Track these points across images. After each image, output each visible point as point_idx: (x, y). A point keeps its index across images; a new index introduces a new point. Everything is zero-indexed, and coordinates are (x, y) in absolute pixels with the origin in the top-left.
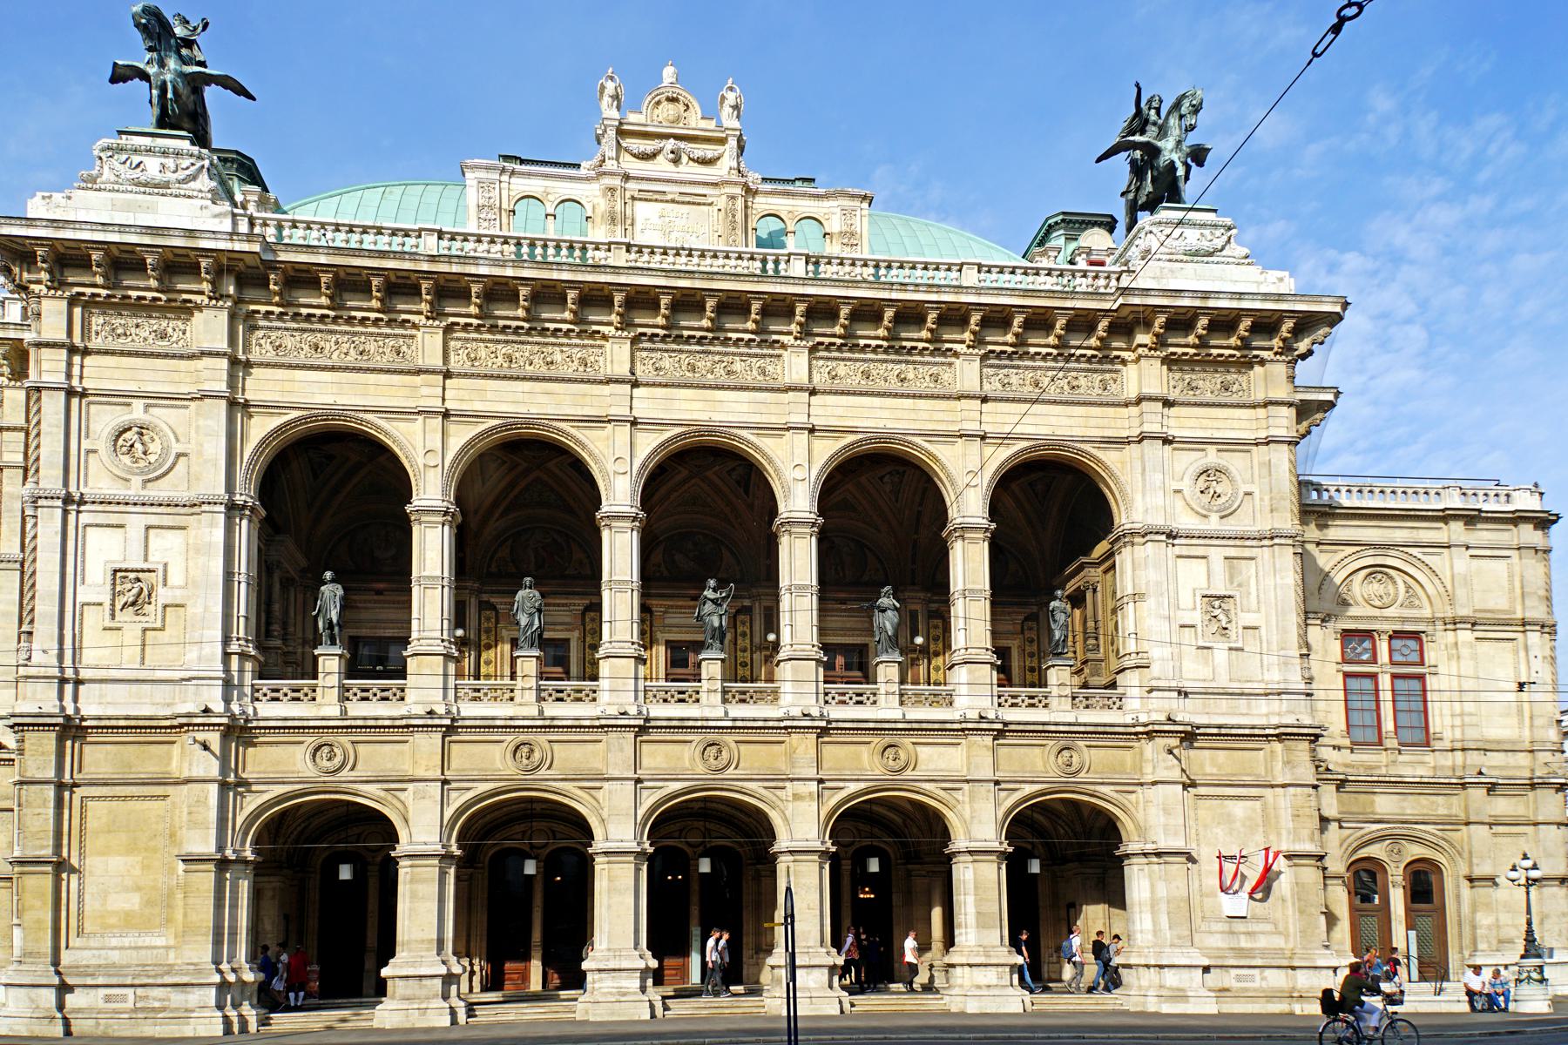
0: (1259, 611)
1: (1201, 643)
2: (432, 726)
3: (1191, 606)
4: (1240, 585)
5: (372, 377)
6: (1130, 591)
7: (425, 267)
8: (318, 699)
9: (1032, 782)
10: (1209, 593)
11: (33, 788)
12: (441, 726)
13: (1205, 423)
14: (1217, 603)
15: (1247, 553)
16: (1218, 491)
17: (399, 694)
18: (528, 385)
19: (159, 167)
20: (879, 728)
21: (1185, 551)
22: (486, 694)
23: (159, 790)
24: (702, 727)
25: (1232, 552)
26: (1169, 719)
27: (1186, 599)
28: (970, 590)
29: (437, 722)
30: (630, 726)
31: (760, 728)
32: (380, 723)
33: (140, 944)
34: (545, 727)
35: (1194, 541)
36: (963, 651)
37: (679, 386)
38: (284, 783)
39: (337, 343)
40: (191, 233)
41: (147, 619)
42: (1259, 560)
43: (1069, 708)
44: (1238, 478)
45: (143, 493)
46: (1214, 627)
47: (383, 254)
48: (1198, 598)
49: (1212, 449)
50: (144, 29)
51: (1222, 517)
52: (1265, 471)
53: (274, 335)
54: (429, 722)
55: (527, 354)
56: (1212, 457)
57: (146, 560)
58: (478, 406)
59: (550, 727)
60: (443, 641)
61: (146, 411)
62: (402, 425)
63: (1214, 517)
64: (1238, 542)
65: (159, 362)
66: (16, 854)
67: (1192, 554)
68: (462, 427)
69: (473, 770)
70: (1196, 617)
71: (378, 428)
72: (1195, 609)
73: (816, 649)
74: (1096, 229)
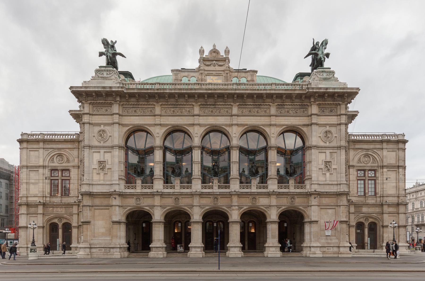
0: (337, 165)
1: (323, 173)
2: (158, 194)
3: (321, 164)
4: (333, 159)
5: (146, 117)
6: (308, 161)
7: (156, 91)
8: (137, 188)
9: (285, 206)
10: (326, 161)
11: (85, 207)
12: (160, 194)
13: (327, 120)
14: (327, 163)
15: (335, 151)
16: (329, 136)
17: (152, 187)
18: (177, 117)
19: (106, 74)
20: (251, 194)
21: (321, 151)
22: (169, 187)
23: (108, 208)
24: (213, 194)
25: (332, 151)
26: (315, 191)
27: (320, 162)
28: (272, 162)
29: (159, 193)
30: (198, 194)
31: (226, 194)
32: (148, 193)
33: (105, 239)
34: (181, 194)
35: (323, 149)
36: (270, 176)
37: (209, 116)
38: (130, 206)
39: (139, 110)
40: (111, 87)
41: (104, 171)
42: (337, 153)
43: (294, 188)
44: (333, 133)
45: (103, 145)
46: (326, 169)
47: (148, 89)
48: (323, 162)
49: (328, 127)
50: (103, 43)
51: (329, 143)
52: (339, 131)
53: (127, 109)
54: (158, 193)
55: (177, 110)
56: (328, 128)
57: (104, 159)
58: (167, 123)
59: (182, 194)
60: (160, 175)
61: (104, 127)
62: (152, 128)
63: (328, 143)
64: (333, 149)
65: (106, 117)
66: (82, 221)
67: (322, 151)
68: (164, 128)
69: (166, 204)
70: (323, 166)
71: (147, 128)
72: (322, 164)
73: (238, 176)
74: (307, 76)
